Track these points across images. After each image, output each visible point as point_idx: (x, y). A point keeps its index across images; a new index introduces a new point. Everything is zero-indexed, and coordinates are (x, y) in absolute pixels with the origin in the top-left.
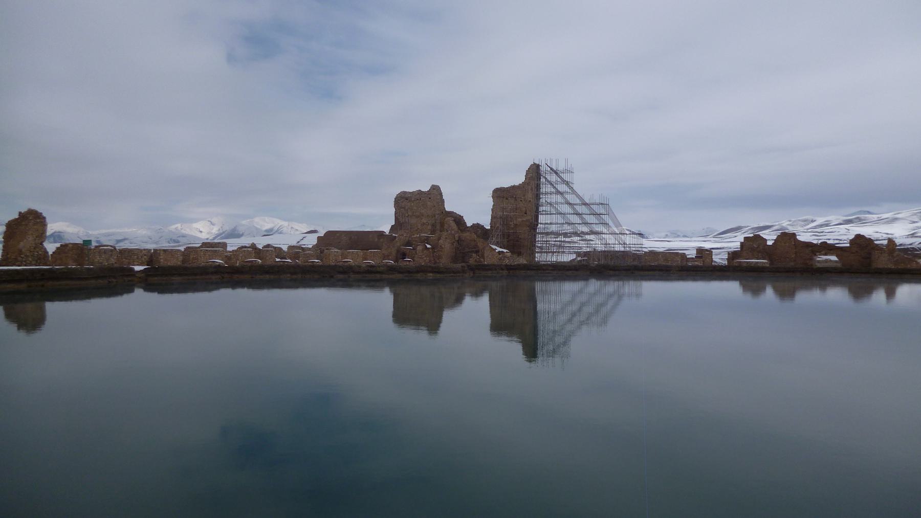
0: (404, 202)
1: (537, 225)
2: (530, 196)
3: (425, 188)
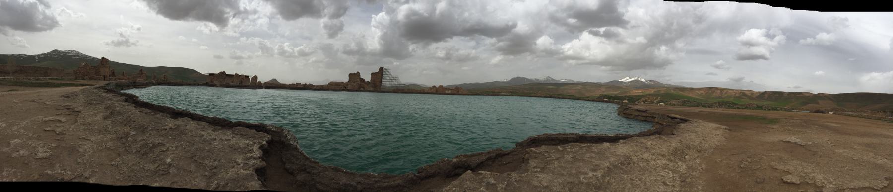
0: (351, 75)
2: (380, 75)
3: (356, 72)
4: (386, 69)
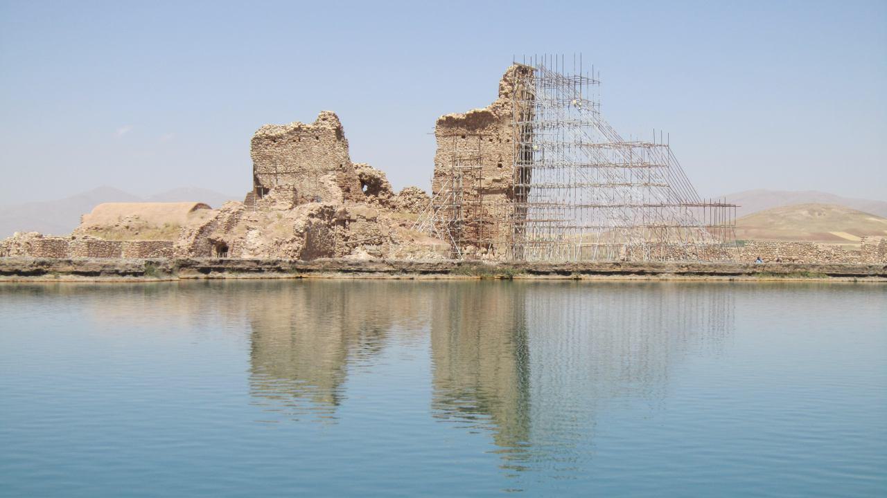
1: (528, 189)
4: (558, 81)
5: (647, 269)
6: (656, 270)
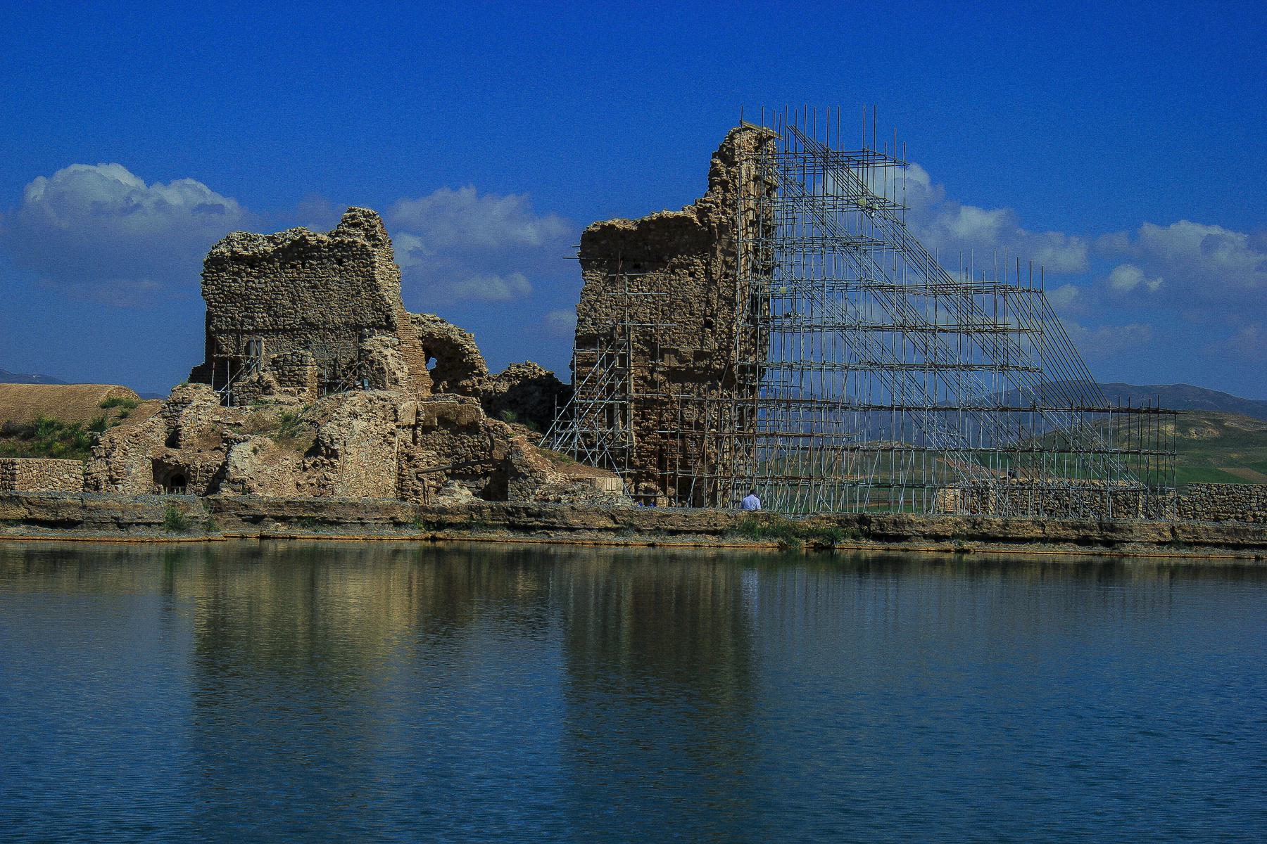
5: (1095, 534)
6: (1118, 536)
